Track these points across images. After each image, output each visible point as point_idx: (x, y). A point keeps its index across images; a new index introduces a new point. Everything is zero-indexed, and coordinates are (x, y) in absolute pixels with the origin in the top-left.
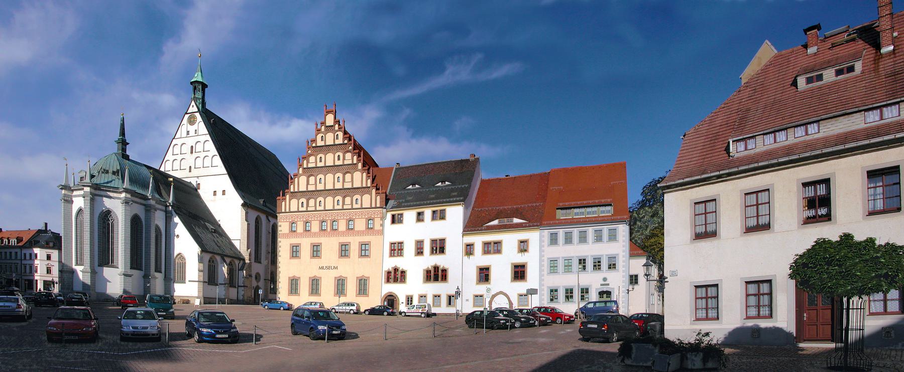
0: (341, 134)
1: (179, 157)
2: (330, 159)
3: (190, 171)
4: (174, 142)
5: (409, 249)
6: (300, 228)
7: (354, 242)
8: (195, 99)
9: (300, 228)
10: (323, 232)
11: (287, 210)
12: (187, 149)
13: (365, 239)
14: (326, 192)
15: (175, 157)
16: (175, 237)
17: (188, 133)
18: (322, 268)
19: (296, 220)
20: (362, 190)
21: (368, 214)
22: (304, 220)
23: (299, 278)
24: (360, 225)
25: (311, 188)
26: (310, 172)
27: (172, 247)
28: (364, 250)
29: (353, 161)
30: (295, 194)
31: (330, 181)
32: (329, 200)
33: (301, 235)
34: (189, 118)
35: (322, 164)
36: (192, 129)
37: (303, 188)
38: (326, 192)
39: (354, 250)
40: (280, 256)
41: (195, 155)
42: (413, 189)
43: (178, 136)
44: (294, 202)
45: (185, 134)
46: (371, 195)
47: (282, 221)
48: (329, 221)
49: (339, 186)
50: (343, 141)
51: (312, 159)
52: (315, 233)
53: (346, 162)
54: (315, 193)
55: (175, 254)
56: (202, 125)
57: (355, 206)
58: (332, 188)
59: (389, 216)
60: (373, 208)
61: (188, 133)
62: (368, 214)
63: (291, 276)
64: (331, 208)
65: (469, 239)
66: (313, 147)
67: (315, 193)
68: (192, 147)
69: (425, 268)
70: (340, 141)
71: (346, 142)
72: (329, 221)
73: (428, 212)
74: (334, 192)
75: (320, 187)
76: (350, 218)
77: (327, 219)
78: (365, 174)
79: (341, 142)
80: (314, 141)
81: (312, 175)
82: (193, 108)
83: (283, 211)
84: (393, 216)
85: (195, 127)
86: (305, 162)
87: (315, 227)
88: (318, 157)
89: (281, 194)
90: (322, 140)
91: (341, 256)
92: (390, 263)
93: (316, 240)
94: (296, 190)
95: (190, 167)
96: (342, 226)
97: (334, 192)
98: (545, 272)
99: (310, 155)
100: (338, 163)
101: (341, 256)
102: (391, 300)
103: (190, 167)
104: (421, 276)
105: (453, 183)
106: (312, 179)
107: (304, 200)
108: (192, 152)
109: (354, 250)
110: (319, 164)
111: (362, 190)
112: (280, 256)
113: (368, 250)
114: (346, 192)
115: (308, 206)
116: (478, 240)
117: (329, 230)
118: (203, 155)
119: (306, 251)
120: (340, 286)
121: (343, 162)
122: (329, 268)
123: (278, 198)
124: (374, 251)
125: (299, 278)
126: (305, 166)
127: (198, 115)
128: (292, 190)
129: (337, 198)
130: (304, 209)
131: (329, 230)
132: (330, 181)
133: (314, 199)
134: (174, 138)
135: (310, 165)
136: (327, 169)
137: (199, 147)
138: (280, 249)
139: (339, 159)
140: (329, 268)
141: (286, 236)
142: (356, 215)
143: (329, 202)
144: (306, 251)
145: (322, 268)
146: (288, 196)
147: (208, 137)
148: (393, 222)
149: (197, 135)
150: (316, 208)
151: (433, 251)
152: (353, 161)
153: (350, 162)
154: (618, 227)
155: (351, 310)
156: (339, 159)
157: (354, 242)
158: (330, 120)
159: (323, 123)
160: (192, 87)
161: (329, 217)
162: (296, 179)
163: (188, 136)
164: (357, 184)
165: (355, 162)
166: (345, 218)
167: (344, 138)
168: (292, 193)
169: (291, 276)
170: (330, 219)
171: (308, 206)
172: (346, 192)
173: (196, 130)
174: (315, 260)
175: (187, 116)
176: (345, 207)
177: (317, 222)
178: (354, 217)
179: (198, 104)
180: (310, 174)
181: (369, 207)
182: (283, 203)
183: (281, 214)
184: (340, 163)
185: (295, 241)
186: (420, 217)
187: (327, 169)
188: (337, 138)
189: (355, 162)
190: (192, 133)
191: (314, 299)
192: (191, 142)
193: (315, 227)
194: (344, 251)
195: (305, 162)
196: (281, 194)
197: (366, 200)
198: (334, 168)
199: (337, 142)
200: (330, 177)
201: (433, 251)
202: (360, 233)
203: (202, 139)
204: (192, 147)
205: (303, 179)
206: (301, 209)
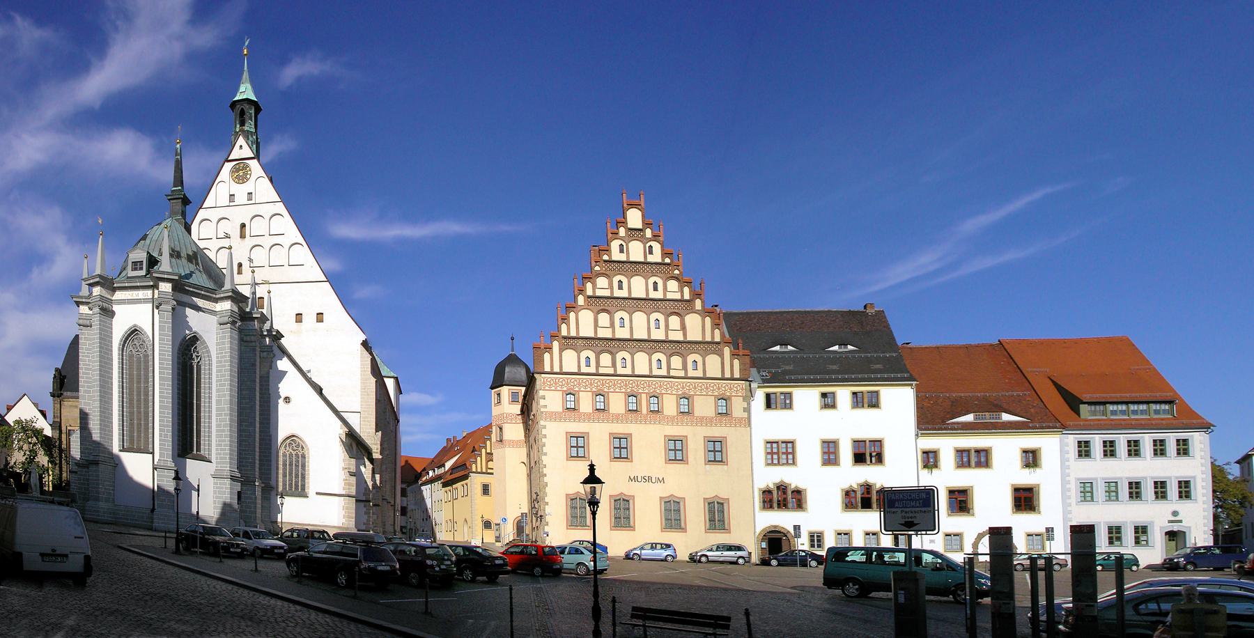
0: (657, 247)
2: (638, 286)
5: (809, 453)
6: (586, 404)
8: (247, 135)
9: (586, 404)
10: (630, 415)
11: (557, 369)
13: (716, 432)
16: (281, 401)
19: (577, 389)
20: (705, 347)
21: (719, 389)
22: (594, 390)
24: (705, 406)
25: (605, 333)
26: (601, 304)
27: (272, 421)
29: (682, 296)
31: (641, 325)
32: (641, 358)
33: (588, 418)
34: (235, 170)
35: (624, 293)
36: (241, 191)
37: (587, 331)
39: (696, 450)
41: (249, 242)
42: (841, 352)
44: (569, 356)
46: (722, 356)
47: (547, 388)
49: (658, 335)
50: (663, 258)
51: (602, 282)
53: (669, 296)
54: (611, 345)
55: (281, 437)
56: (265, 183)
57: (691, 373)
58: (664, 338)
59: (760, 395)
60: (727, 379)
62: (719, 389)
63: (571, 492)
65: (930, 443)
66: (605, 261)
68: (243, 226)
70: (656, 257)
71: (667, 260)
73: (843, 394)
74: (649, 345)
75: (622, 333)
76: (684, 393)
77: (640, 391)
78: (708, 320)
79: (659, 260)
80: (608, 251)
81: (604, 311)
83: (547, 369)
84: (768, 396)
85: (248, 187)
87: (617, 404)
88: (616, 280)
90: (621, 251)
93: (620, 428)
94: (573, 334)
96: (670, 406)
97: (649, 345)
98: (1073, 500)
99: (600, 274)
100: (653, 295)
102: (775, 542)
105: (861, 348)
106: (604, 318)
107: (592, 355)
108: (243, 236)
109: (696, 450)
110: (617, 293)
111: (705, 347)
113: (709, 451)
115: (598, 365)
116: (947, 445)
117: (644, 411)
120: (673, 514)
121: (665, 295)
124: (732, 453)
126: (589, 292)
128: (564, 332)
129: (691, 358)
131: (644, 411)
132: (641, 325)
133: (611, 353)
136: (635, 304)
137: (256, 227)
138: (544, 440)
139: (655, 289)
141: (554, 416)
142: (661, 387)
143: (642, 362)
148: (769, 403)
149: (253, 202)
150: (615, 370)
151: (859, 458)
152: (682, 296)
153: (678, 296)
154: (1094, 438)
155: (579, 564)
156: (655, 289)
158: (634, 218)
159: (624, 223)
161: (644, 387)
162: (572, 315)
163: (231, 204)
164: (694, 334)
165: (687, 296)
166: (674, 392)
167: (665, 254)
168: (565, 338)
170: (647, 391)
175: (228, 167)
176: (673, 373)
178: (692, 393)
180: (602, 308)
181: (720, 376)
182: (547, 356)
183: (543, 375)
184: (659, 295)
186: (828, 402)
187: (635, 304)
188: (651, 253)
189: (687, 296)
190: (241, 198)
192: (240, 215)
193: (617, 404)
194: (676, 451)
195: (589, 286)
197: (713, 364)
198: (646, 304)
199: (650, 259)
200: (639, 317)
201: (859, 458)
203: (267, 210)
204: (243, 226)
206: (584, 369)
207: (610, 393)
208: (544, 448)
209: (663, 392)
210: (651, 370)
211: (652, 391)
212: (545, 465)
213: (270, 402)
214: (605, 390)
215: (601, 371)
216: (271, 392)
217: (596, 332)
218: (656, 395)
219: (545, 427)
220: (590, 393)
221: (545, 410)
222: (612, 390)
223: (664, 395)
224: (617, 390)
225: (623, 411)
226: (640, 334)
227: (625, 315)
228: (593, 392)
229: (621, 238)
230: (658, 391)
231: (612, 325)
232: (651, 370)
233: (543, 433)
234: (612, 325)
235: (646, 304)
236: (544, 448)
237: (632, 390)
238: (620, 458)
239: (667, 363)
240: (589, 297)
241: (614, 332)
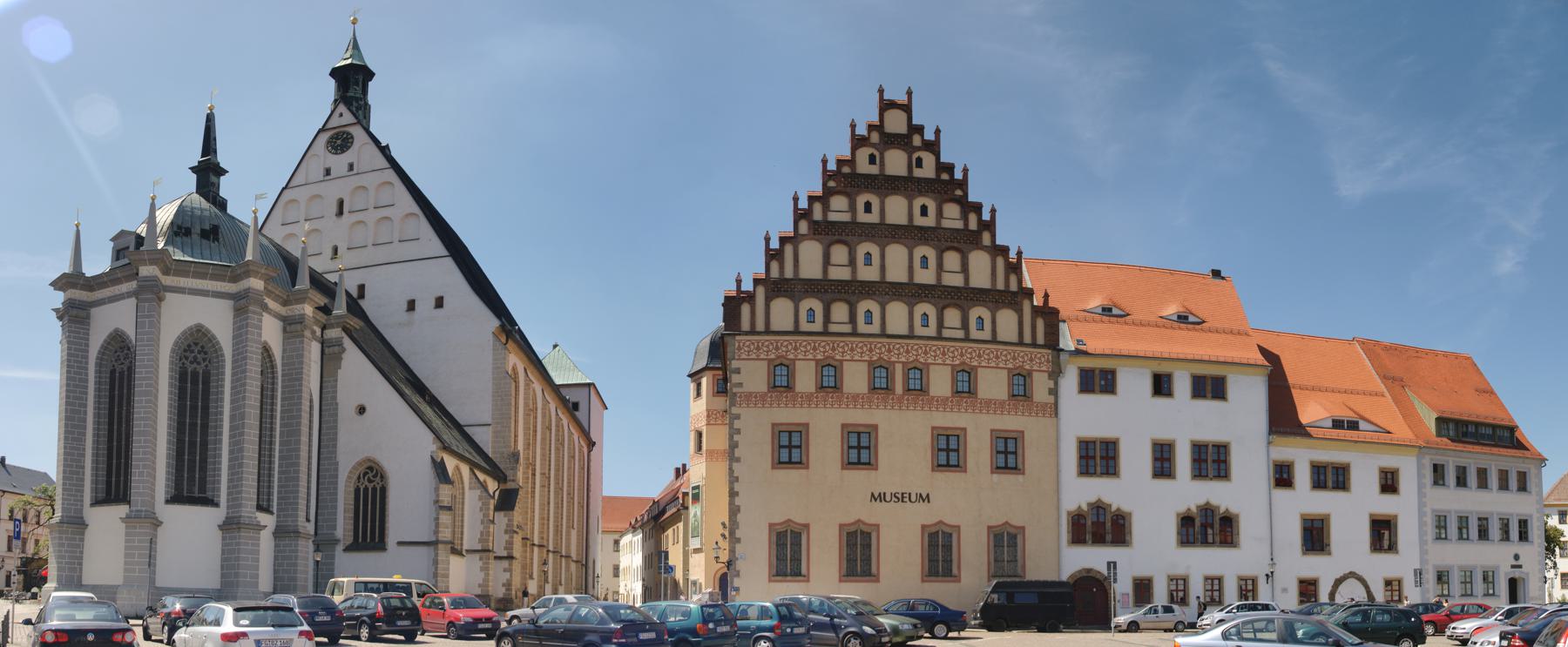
6: (805, 379)
7: (978, 430)
9: (805, 379)
14: (885, 291)
17: (328, 172)
18: (881, 497)
23: (807, 526)
25: (840, 273)
28: (1008, 454)
31: (897, 262)
36: (339, 162)
38: (885, 291)
44: (782, 314)
48: (899, 368)
52: (855, 398)
61: (328, 172)
64: (904, 330)
67: (852, 291)
68: (341, 203)
69: (1182, 509)
72: (899, 368)
75: (868, 274)
77: (893, 359)
86: (818, 207)
87: (856, 378)
91: (939, 466)
92: (1081, 492)
93: (859, 416)
101: (939, 466)
104: (1171, 529)
106: (839, 253)
107: (817, 306)
114: (941, 295)
117: (899, 389)
119: (826, 446)
122: (901, 498)
125: (807, 526)
131: (899, 389)
132: (897, 262)
133: (848, 302)
135: (833, 217)
140: (901, 498)
143: (897, 317)
144: (826, 446)
145: (881, 497)
157: (978, 430)
161: (899, 356)
163: (328, 177)
169: (778, 519)
170: (903, 359)
172: (941, 295)
174: (858, 476)
177: (863, 368)
185: (788, 415)
191: (853, 592)
193: (856, 378)
202: (990, 406)
204: (341, 203)
207: (845, 363)
208: (736, 450)
209: (930, 361)
210: (911, 327)
211: (911, 359)
212: (737, 478)
213: (337, 415)
214: (838, 357)
215: (833, 328)
216: (338, 401)
217: (825, 271)
218: (920, 366)
219: (738, 417)
220: (813, 364)
221: (740, 390)
222: (848, 357)
223: (932, 367)
224: (856, 358)
225: (865, 390)
226: (897, 274)
227: (874, 250)
228: (817, 361)
229: (873, 145)
230: (922, 360)
231: (852, 262)
232: (911, 327)
233: (735, 427)
234: (852, 262)
235: (909, 234)
236: (736, 450)
237: (880, 358)
238: (859, 463)
239: (938, 319)
241: (854, 272)
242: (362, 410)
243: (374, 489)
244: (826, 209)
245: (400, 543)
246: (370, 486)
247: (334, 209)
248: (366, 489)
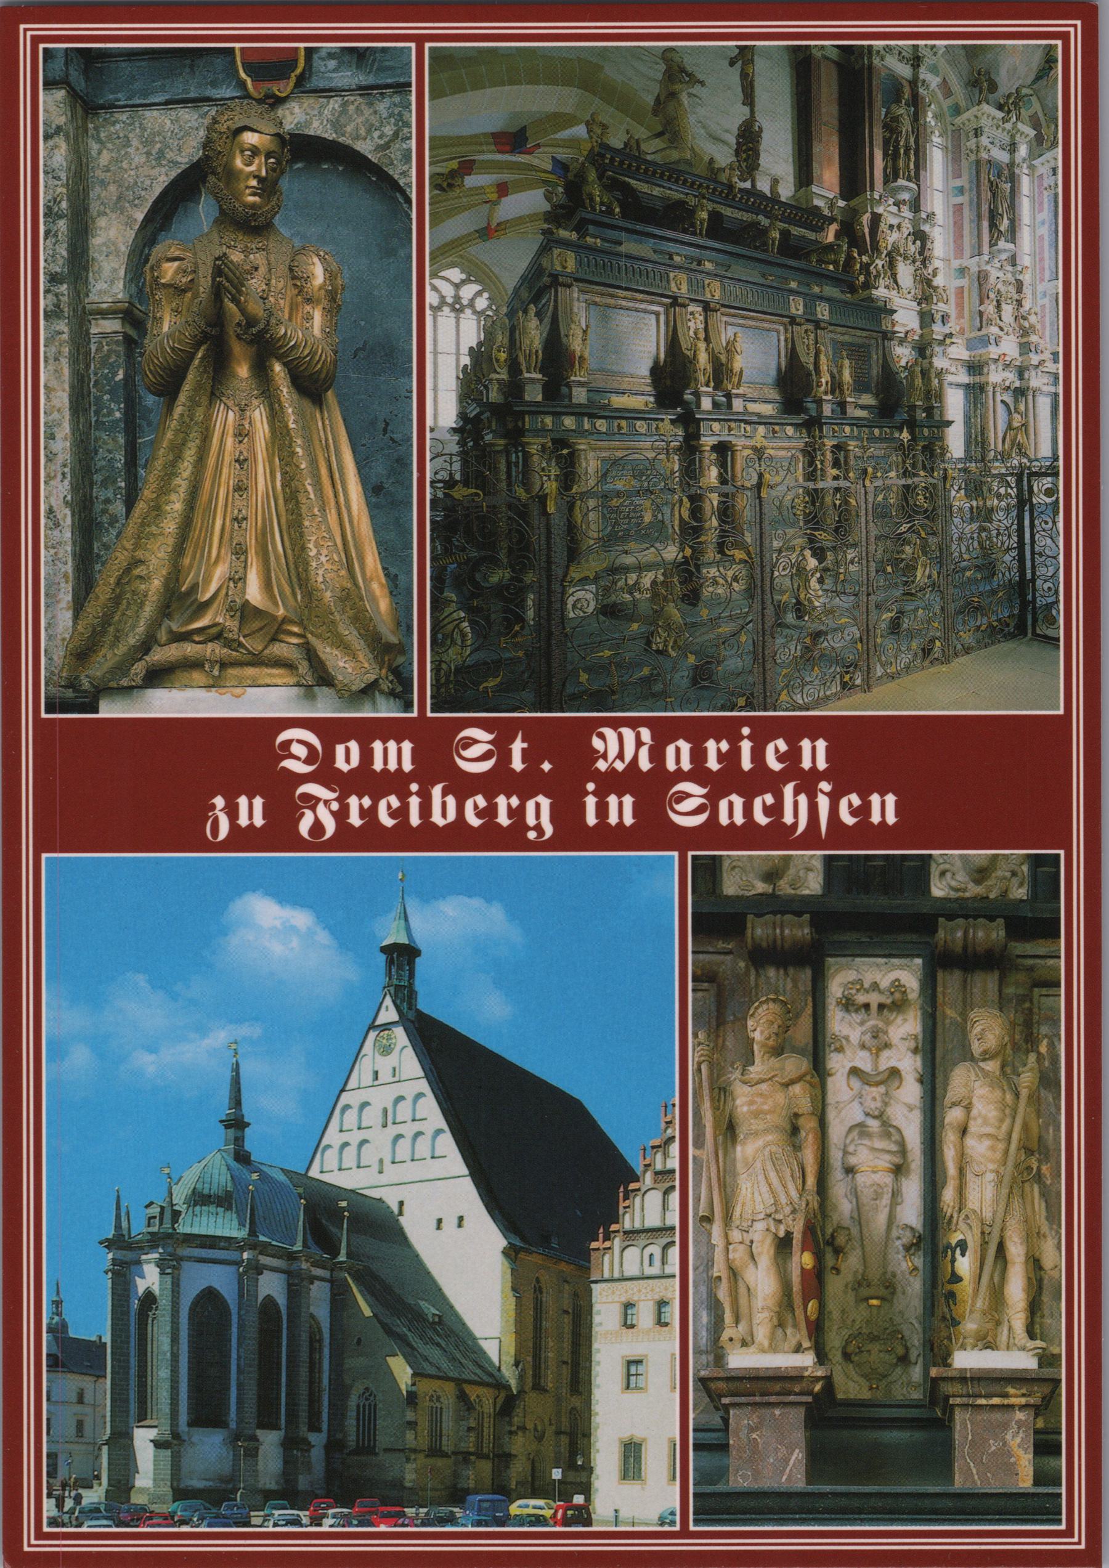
1: (355, 1138)
3: (381, 1172)
4: (345, 1099)
11: (616, 1275)
12: (372, 1116)
15: (345, 1137)
17: (376, 1073)
30: (631, 1234)
36: (385, 1065)
37: (653, 1220)
40: (598, 1387)
41: (392, 1131)
43: (352, 1084)
44: (632, 1254)
45: (367, 1079)
47: (604, 1300)
82: (389, 1014)
83: (606, 1275)
85: (392, 1060)
89: (601, 1236)
94: (638, 1225)
95: (381, 1161)
103: (381, 1161)
107: (656, 1250)
108: (385, 1126)
112: (598, 1387)
115: (664, 1262)
118: (409, 1130)
123: (594, 1245)
126: (659, 1167)
127: (399, 1033)
128: (627, 1226)
130: (655, 1270)
134: (343, 1090)
146: (617, 1243)
147: (424, 1086)
149: (396, 1079)
160: (382, 958)
163: (376, 1083)
168: (625, 1233)
171: (664, 1262)
173: (394, 1069)
175: (372, 1035)
179: (398, 1002)
182: (607, 1258)
192: (380, 1098)
195: (659, 1156)
196: (601, 1236)
203: (409, 1090)
204: (385, 1111)
205: (654, 1199)
206: (649, 1271)
240: (657, 1173)
242: (359, 1341)
243: (370, 1405)
244: (666, 1155)
245: (386, 1450)
246: (367, 1403)
247: (380, 1120)
248: (364, 1405)
